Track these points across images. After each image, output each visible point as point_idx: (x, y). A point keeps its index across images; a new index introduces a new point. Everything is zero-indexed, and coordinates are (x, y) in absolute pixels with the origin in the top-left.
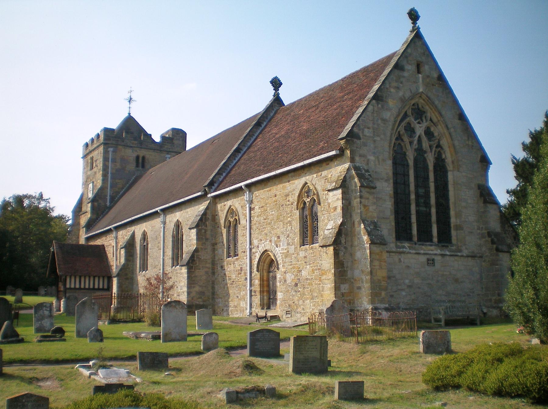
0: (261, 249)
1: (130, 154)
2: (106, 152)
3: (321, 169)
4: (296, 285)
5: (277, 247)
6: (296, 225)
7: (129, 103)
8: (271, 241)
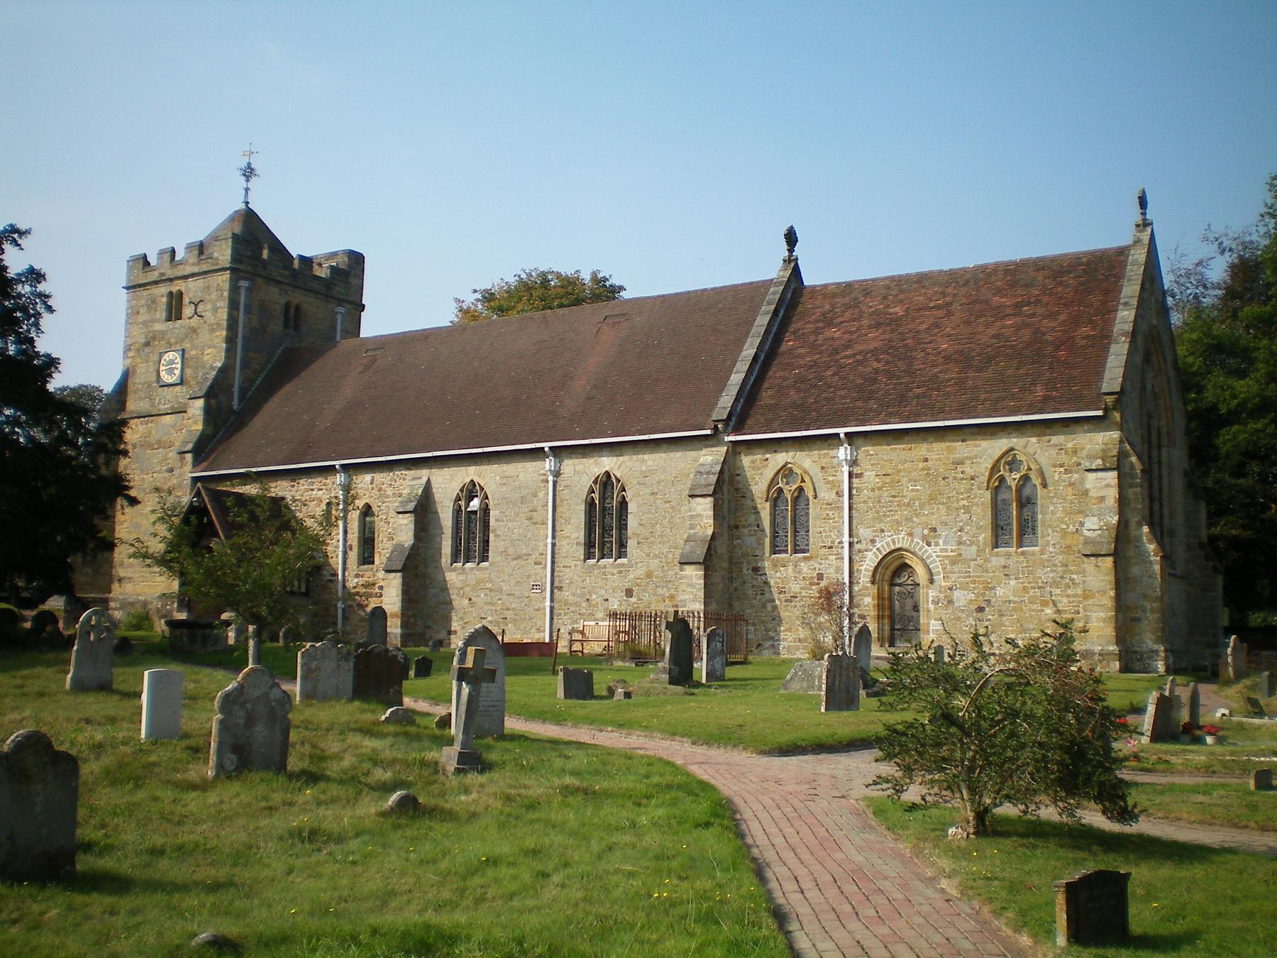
0: (885, 544)
1: (275, 297)
2: (234, 289)
3: (1048, 431)
4: (981, 609)
5: (929, 544)
6: (982, 515)
7: (244, 178)
8: (910, 534)
